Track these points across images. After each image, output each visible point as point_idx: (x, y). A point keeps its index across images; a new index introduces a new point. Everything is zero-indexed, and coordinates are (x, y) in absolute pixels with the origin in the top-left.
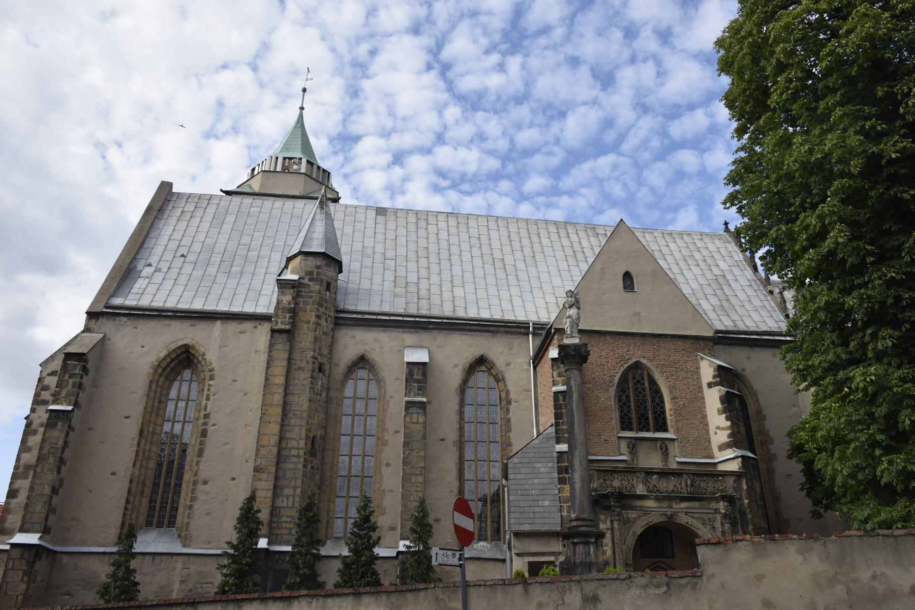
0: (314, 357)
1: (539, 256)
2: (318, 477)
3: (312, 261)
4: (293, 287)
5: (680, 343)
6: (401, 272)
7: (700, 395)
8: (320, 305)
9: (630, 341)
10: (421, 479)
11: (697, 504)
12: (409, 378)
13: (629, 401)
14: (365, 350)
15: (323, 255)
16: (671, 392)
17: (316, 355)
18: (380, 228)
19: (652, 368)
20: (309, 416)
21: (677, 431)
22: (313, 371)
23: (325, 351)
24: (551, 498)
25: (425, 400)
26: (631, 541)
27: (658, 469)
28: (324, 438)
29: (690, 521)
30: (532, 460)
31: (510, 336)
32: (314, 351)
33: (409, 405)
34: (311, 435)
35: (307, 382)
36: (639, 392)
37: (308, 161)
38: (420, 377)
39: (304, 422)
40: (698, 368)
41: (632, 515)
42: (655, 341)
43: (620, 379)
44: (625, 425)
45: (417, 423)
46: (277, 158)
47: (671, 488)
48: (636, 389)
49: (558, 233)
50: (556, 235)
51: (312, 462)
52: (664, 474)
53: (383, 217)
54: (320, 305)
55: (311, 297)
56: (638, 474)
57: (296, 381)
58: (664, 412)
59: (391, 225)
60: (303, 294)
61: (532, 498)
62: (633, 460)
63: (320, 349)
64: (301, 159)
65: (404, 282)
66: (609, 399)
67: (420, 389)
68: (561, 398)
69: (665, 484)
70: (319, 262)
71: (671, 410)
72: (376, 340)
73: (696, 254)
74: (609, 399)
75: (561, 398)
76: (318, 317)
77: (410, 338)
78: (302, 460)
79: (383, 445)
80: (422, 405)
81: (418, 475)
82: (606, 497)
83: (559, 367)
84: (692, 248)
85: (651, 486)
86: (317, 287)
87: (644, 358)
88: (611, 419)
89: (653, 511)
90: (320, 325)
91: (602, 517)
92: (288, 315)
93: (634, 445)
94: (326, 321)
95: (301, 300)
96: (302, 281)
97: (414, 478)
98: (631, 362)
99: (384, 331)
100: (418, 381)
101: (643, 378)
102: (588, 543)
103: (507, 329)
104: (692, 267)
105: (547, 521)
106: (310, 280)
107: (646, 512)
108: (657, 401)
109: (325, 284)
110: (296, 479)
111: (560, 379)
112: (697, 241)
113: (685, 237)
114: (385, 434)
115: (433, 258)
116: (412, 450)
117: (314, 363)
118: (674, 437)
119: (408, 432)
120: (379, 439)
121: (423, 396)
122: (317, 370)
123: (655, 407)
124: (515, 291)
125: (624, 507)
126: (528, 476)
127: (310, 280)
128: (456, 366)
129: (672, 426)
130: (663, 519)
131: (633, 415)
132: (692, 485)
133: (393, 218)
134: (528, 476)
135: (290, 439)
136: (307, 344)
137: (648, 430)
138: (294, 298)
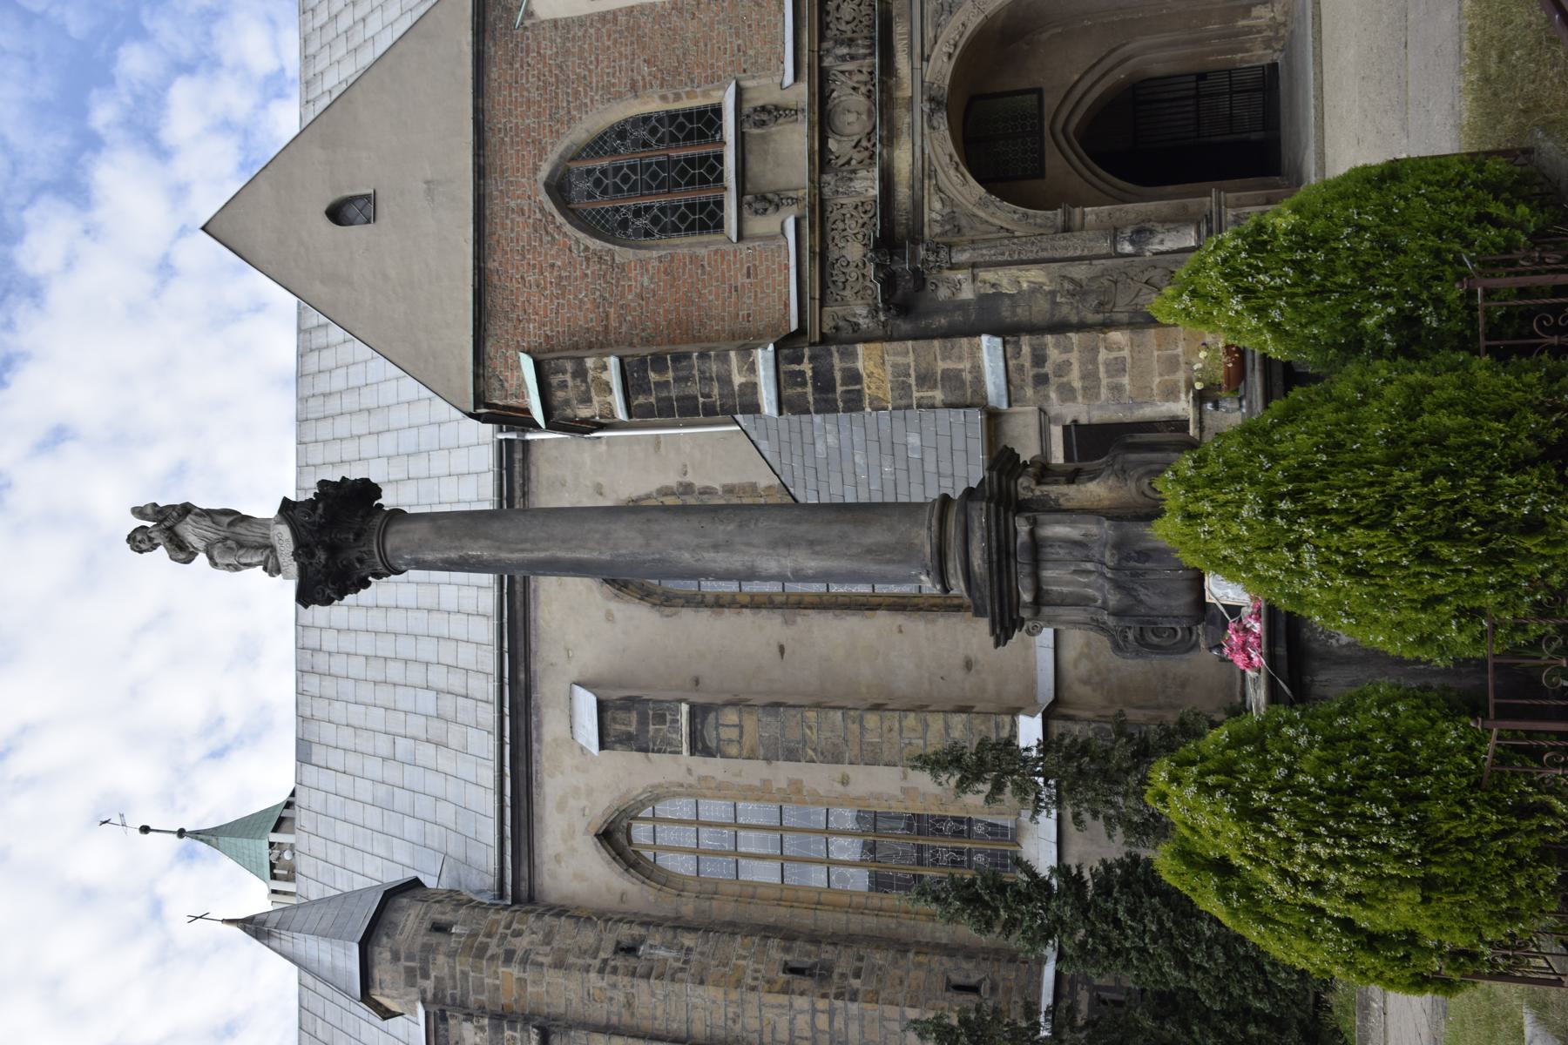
0: (601, 971)
1: (368, 400)
2: (879, 958)
3: (383, 971)
4: (443, 1018)
5: (494, 72)
6: (416, 725)
7: (622, 19)
8: (481, 952)
9: (495, 207)
10: (872, 720)
11: (900, 30)
12: (637, 743)
13: (648, 209)
14: (586, 832)
15: (366, 945)
16: (619, 96)
17: (597, 963)
18: (336, 759)
19: (560, 148)
20: (738, 984)
21: (715, 80)
22: (633, 974)
23: (588, 937)
24: (898, 424)
25: (685, 708)
26: (1003, 214)
27: (811, 138)
28: (788, 935)
29: (943, 48)
30: (809, 462)
31: (533, 485)
32: (587, 969)
33: (699, 746)
34: (783, 977)
35: (660, 988)
36: (624, 181)
37: (275, 830)
38: (634, 717)
39: (752, 997)
40: (555, 23)
41: (934, 209)
42: (493, 140)
43: (594, 234)
44: (709, 219)
45: (740, 727)
46: (274, 892)
47: (859, 101)
48: (618, 189)
49: (320, 349)
50: (325, 353)
51: (843, 976)
52: (824, 121)
53: (315, 748)
54: (481, 952)
55: (464, 974)
56: (826, 190)
57: (659, 1012)
58: (672, 116)
59: (328, 733)
60: (458, 992)
61: (902, 475)
62: (796, 201)
63: (582, 953)
64: (271, 845)
65: (435, 723)
66: (643, 264)
67: (661, 719)
68: (641, 400)
69: (851, 118)
70: (382, 955)
71: (664, 98)
72: (561, 806)
73: (345, 21)
74: (643, 264)
75: (641, 400)
76: (509, 957)
77: (550, 727)
78: (839, 1004)
79: (799, 791)
80: (698, 713)
81: (862, 726)
82: (889, 282)
83: (567, 402)
84: (330, 33)
85: (857, 156)
86: (441, 959)
87: (536, 169)
88: (694, 259)
89: (924, 151)
90: (527, 953)
91: (943, 293)
92: (508, 1033)
93: (758, 199)
94: (518, 934)
95: (472, 998)
96: (429, 996)
97: (872, 738)
98: (550, 206)
99: (540, 786)
100: (643, 721)
101: (590, 172)
102: (1036, 545)
103: (518, 493)
104: (369, 33)
105: (959, 444)
106: (426, 976)
107: (925, 172)
108: (643, 133)
109: (436, 938)
110: (883, 1018)
111: (595, 399)
112: (317, 23)
113: (311, 50)
114: (775, 785)
115: (386, 647)
116: (804, 741)
117: (615, 970)
118: (731, 90)
119: (762, 752)
120: (788, 800)
121: (678, 711)
122: (632, 961)
123: (661, 141)
124: (439, 464)
125: (916, 236)
126: (849, 479)
127: (426, 976)
128: (609, 617)
129: (706, 94)
130: (942, 121)
131: (681, 197)
132: (851, 42)
133: (314, 726)
134: (849, 479)
135: (791, 1031)
136: (573, 985)
137: (720, 158)
138: (469, 1017)
